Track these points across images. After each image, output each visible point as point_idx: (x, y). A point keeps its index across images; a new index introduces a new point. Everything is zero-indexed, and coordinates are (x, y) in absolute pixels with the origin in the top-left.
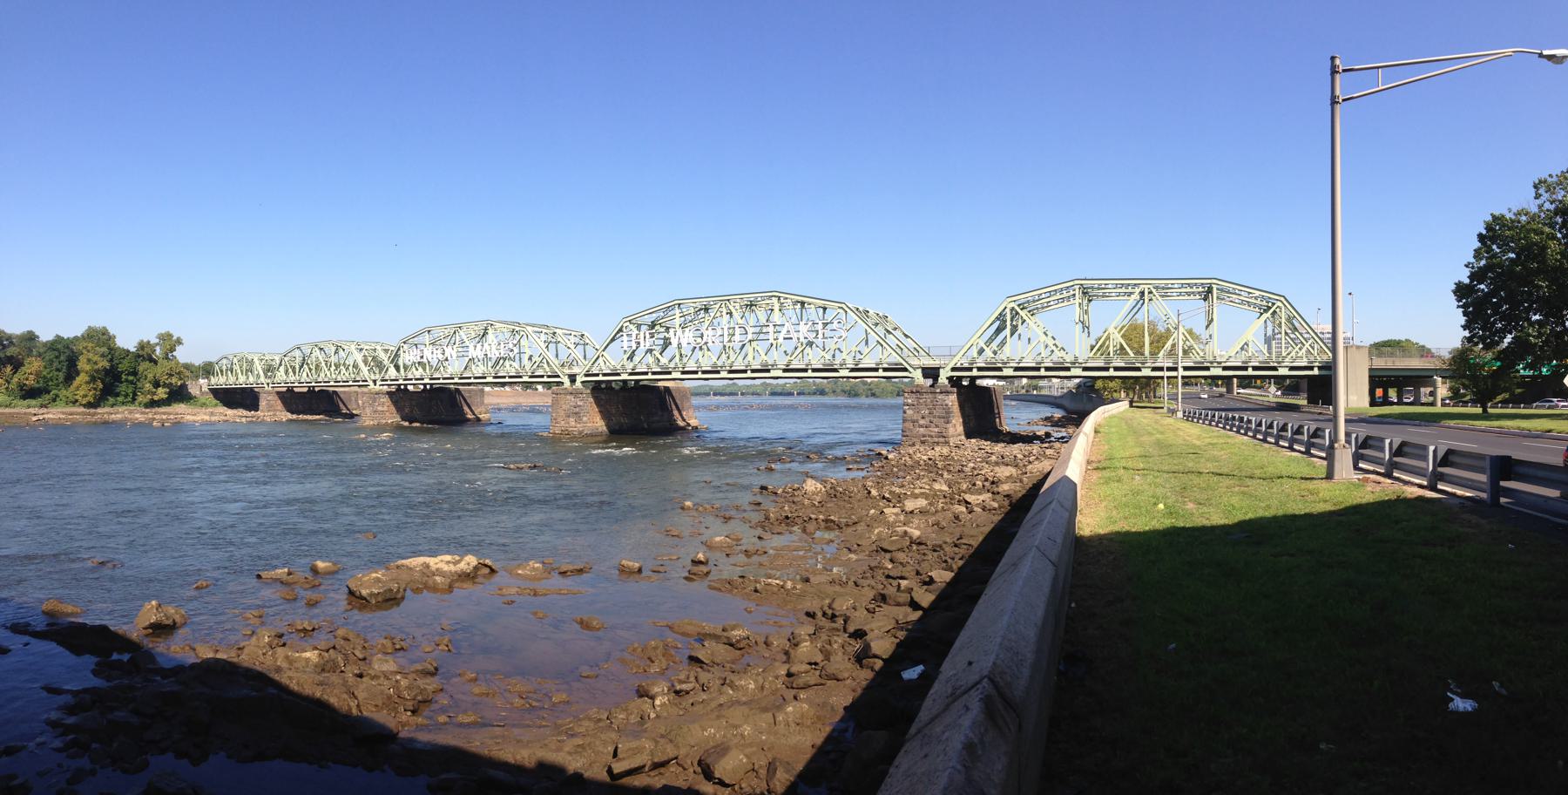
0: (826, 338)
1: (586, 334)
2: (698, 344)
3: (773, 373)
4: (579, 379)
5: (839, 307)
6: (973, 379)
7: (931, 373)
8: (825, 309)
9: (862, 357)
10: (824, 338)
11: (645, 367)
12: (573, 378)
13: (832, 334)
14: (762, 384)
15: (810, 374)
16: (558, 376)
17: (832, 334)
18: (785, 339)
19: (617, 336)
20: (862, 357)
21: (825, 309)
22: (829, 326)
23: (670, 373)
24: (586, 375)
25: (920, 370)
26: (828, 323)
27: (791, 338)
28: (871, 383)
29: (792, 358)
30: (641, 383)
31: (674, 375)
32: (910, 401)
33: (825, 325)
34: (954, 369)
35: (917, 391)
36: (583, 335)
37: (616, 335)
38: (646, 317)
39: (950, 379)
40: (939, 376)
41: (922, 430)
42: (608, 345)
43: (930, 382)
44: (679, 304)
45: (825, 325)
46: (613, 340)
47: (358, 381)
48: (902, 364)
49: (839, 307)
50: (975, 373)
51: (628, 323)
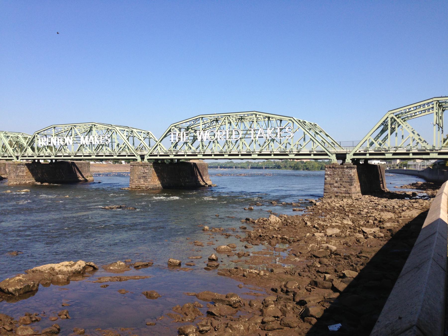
0: (282, 137)
1: (150, 132)
2: (212, 139)
4: (146, 158)
5: (289, 120)
6: (366, 160)
7: (341, 157)
8: (281, 121)
9: (302, 148)
10: (280, 137)
12: (142, 157)
13: (285, 134)
14: (247, 162)
15: (272, 157)
16: (134, 156)
19: (168, 134)
20: (302, 148)
21: (281, 121)
22: (283, 131)
23: (196, 155)
24: (150, 156)
25: (335, 155)
26: (283, 129)
27: (263, 137)
28: (306, 162)
29: (263, 148)
30: (181, 161)
31: (199, 157)
32: (329, 173)
33: (281, 130)
34: (355, 154)
35: (333, 167)
36: (148, 133)
38: (184, 124)
39: (353, 160)
40: (346, 158)
41: (336, 189)
42: (162, 139)
43: (341, 161)
44: (202, 118)
45: (281, 130)
46: (165, 136)
47: (6, 157)
48: (324, 152)
49: (289, 120)
50: (368, 156)
51: (174, 127)
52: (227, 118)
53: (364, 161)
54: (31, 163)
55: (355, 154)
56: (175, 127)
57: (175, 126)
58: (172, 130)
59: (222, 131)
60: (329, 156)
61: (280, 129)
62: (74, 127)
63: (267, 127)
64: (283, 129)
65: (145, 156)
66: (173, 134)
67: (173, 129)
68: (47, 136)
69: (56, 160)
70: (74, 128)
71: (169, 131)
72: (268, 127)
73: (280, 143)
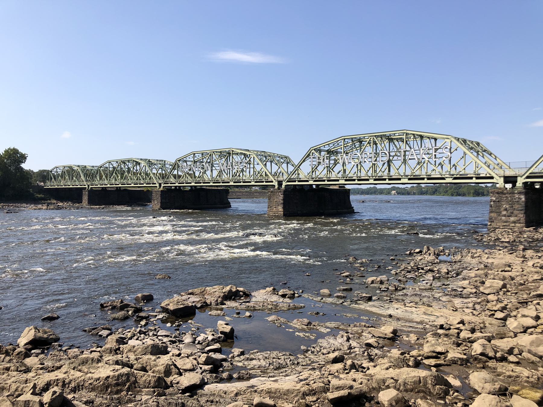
0: (437, 158)
2: (355, 163)
3: (403, 181)
4: (284, 184)
7: (511, 180)
8: (436, 139)
10: (435, 158)
11: (438, 174)
13: (441, 155)
17: (441, 155)
18: (410, 159)
21: (436, 139)
22: (439, 151)
23: (338, 180)
24: (288, 181)
25: (502, 179)
26: (437, 149)
27: (414, 159)
30: (320, 187)
31: (403, 181)
32: (494, 199)
34: (528, 177)
35: (501, 192)
37: (305, 159)
39: (525, 184)
40: (517, 182)
41: (503, 218)
43: (509, 186)
44: (345, 139)
45: (436, 150)
51: (313, 151)
53: (540, 185)
55: (528, 177)
57: (315, 149)
58: (311, 154)
60: (524, 179)
63: (420, 147)
69: (317, 185)
72: (421, 147)
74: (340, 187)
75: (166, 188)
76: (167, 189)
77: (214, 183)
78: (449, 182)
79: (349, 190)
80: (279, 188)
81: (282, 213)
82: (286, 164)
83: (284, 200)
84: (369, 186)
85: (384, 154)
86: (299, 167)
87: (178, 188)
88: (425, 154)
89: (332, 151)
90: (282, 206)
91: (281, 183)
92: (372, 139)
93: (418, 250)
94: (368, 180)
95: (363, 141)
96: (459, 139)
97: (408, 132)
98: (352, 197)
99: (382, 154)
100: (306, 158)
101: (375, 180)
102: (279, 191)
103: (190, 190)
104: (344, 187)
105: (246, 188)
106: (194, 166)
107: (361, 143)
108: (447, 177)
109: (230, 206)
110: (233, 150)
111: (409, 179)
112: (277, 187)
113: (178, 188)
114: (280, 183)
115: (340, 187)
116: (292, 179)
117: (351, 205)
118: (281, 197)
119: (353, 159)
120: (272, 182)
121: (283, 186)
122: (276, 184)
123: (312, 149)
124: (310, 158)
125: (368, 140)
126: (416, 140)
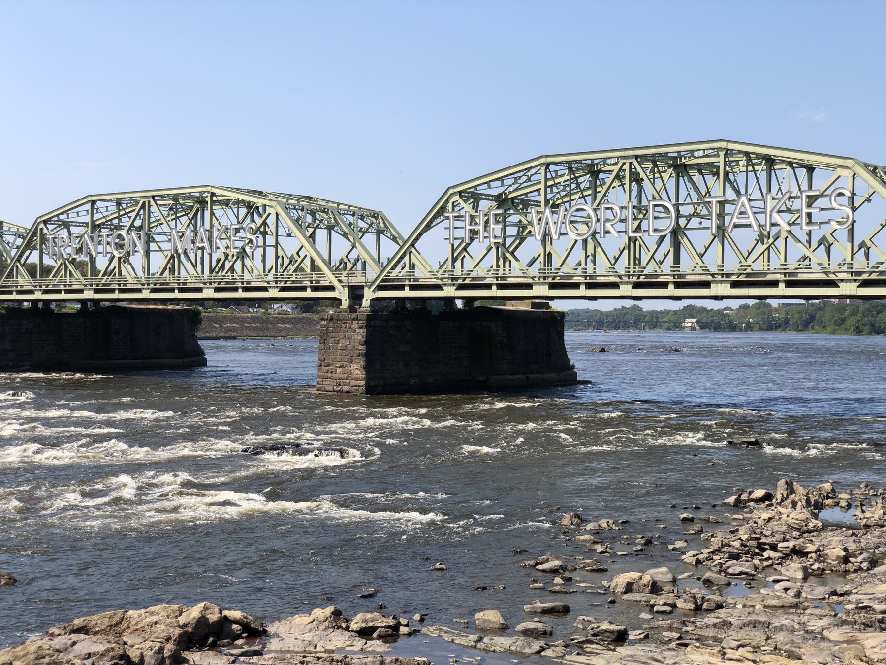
0: (815, 223)
2: (579, 235)
4: (369, 295)
8: (810, 169)
10: (810, 223)
11: (818, 269)
12: (356, 293)
13: (825, 216)
14: (742, 307)
15: (781, 290)
17: (825, 216)
19: (438, 220)
21: (810, 169)
22: (821, 202)
23: (529, 286)
24: (381, 288)
26: (816, 198)
27: (749, 226)
30: (477, 304)
31: (715, 290)
37: (431, 221)
44: (548, 165)
45: (812, 200)
51: (456, 198)
52: (631, 163)
54: (688, 320)
56: (461, 197)
57: (460, 193)
58: (450, 205)
59: (611, 209)
61: (808, 197)
62: (151, 199)
63: (765, 191)
64: (820, 199)
65: (366, 289)
66: (456, 217)
67: (453, 203)
68: (71, 228)
69: (468, 301)
70: (152, 203)
71: (441, 208)
73: (807, 245)
74: (534, 305)
75: (6, 305)
76: (5, 308)
77: (154, 291)
78: (848, 293)
79: (562, 315)
80: (352, 309)
81: (363, 383)
82: (374, 236)
83: (367, 343)
84: (618, 304)
85: (661, 209)
86: (413, 245)
87: (40, 305)
88: (779, 212)
89: (513, 199)
90: (362, 361)
91: (358, 292)
92: (626, 167)
93: (759, 493)
94: (615, 285)
95: (600, 171)
96: (876, 168)
97: (731, 146)
98: (571, 337)
99: (657, 209)
100: (434, 218)
101: (637, 286)
102: (354, 315)
103: (79, 311)
104: (547, 306)
105: (253, 307)
106: (92, 238)
107: (597, 178)
108: (842, 280)
109: (204, 363)
110: (214, 190)
111: (735, 285)
112: (345, 304)
113: (40, 305)
114: (356, 293)
115: (534, 305)
116: (394, 280)
117: (568, 360)
118: (359, 334)
119: (572, 222)
120: (332, 288)
121: (366, 303)
122: (342, 294)
123: (451, 191)
124: (447, 218)
125: (616, 168)
126: (755, 171)
